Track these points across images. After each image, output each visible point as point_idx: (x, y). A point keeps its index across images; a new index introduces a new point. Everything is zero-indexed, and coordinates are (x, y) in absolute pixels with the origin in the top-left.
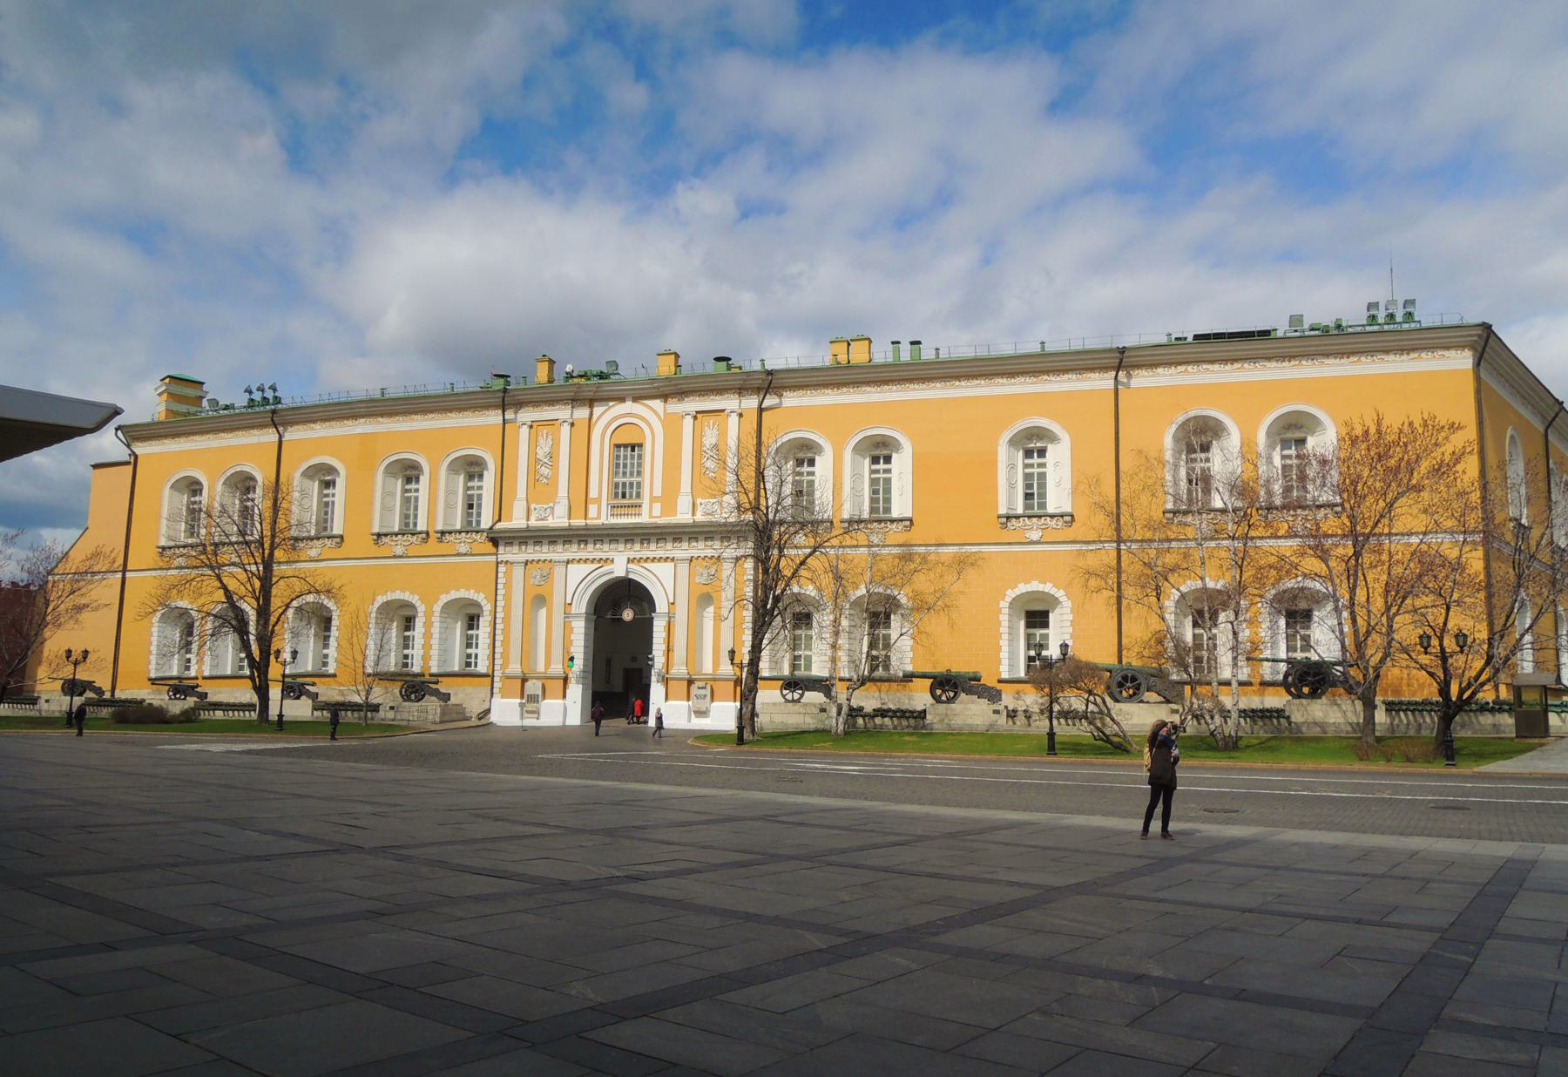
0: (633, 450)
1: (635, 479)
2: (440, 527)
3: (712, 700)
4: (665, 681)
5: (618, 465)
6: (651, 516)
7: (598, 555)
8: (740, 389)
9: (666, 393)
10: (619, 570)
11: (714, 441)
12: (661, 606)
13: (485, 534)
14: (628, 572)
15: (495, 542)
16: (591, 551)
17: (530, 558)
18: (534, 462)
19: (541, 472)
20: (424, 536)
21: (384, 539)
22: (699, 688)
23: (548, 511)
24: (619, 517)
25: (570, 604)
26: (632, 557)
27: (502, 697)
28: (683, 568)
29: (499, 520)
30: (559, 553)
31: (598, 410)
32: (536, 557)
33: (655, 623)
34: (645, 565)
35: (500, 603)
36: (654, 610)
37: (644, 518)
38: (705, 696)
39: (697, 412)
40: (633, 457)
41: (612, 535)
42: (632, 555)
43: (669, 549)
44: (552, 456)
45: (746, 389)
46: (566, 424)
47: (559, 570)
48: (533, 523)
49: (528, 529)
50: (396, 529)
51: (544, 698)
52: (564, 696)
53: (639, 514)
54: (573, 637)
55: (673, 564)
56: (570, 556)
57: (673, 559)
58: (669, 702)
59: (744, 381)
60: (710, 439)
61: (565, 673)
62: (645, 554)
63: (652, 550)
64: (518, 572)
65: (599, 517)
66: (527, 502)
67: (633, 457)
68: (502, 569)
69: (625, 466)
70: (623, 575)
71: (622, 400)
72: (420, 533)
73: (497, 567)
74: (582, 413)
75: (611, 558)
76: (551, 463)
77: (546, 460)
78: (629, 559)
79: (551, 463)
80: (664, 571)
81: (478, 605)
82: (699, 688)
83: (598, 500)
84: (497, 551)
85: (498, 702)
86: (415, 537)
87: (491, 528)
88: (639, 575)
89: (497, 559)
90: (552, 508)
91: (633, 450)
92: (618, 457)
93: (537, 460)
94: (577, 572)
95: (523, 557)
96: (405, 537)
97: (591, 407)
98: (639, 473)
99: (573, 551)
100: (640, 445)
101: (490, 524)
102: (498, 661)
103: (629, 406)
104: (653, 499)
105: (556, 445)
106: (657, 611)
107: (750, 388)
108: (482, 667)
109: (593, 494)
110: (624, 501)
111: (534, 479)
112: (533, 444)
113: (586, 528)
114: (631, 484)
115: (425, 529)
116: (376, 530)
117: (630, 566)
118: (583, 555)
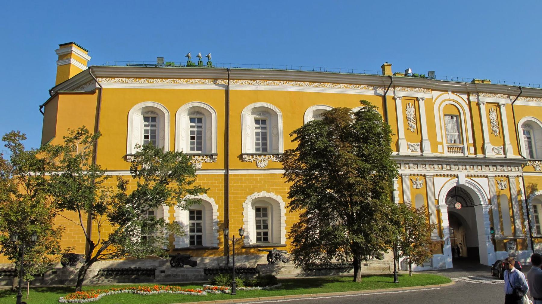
7: (449, 173)
9: (469, 91)
10: (463, 181)
16: (446, 170)
19: (411, 125)
30: (429, 171)
32: (416, 172)
43: (485, 171)
52: (443, 252)
56: (435, 173)
57: (487, 177)
58: (497, 252)
62: (473, 173)
63: (477, 170)
65: (443, 153)
80: (483, 182)
83: (441, 143)
99: (437, 170)
109: (439, 140)
112: (405, 109)
118: (442, 172)
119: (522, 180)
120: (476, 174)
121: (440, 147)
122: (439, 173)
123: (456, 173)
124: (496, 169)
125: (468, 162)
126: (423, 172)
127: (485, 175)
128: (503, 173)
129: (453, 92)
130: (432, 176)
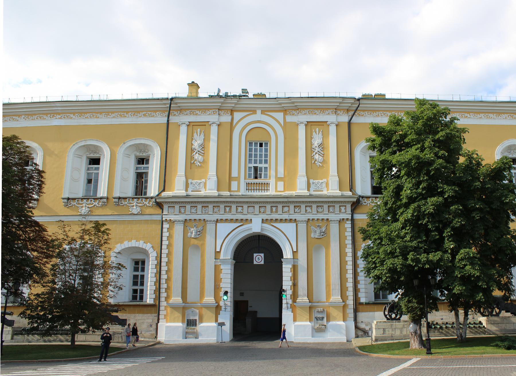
0: (261, 145)
1: (263, 165)
2: (117, 194)
3: (328, 320)
4: (293, 308)
5: (250, 155)
6: (276, 191)
7: (240, 217)
8: (336, 109)
11: (320, 141)
12: (287, 254)
13: (154, 200)
14: (262, 229)
15: (160, 205)
17: (188, 217)
18: (190, 150)
20: (105, 200)
21: (73, 203)
22: (318, 312)
23: (202, 185)
24: (258, 191)
25: (219, 252)
26: (265, 218)
27: (167, 322)
28: (303, 227)
29: (164, 190)
31: (237, 116)
32: (193, 217)
33: (284, 266)
34: (274, 224)
35: (165, 251)
36: (283, 257)
37: (272, 192)
38: (323, 318)
39: (307, 122)
40: (261, 151)
41: (251, 202)
42: (265, 217)
44: (203, 146)
45: (340, 110)
46: (214, 125)
47: (210, 227)
48: (190, 193)
49: (187, 196)
50: (80, 195)
51: (201, 321)
53: (267, 190)
54: (222, 276)
55: (295, 224)
56: (219, 217)
59: (338, 106)
60: (317, 141)
61: (216, 303)
62: (275, 216)
64: (179, 229)
65: (238, 190)
66: (186, 178)
67: (261, 151)
68: (166, 226)
69: (256, 156)
70: (259, 231)
71: (254, 112)
72: (101, 198)
73: (162, 224)
74: (226, 118)
75: (249, 218)
76: (203, 152)
77: (199, 150)
78: (263, 220)
79: (203, 152)
80: (289, 229)
81: (145, 252)
82: (318, 312)
83: (238, 179)
84: (163, 212)
85: (163, 325)
86: (98, 201)
87: (158, 196)
88: (271, 231)
89: (162, 218)
90: (205, 184)
91: (261, 145)
92: (250, 150)
93: (192, 150)
94: (224, 229)
95: (182, 217)
96: (89, 202)
97: (232, 114)
98: (266, 161)
100: (266, 144)
101: (157, 193)
102: (164, 295)
103: (258, 116)
104: (278, 179)
105: (207, 139)
106: (284, 257)
107: (342, 109)
108: (149, 299)
109: (234, 174)
110: (256, 181)
111: (190, 164)
113: (231, 196)
114: (261, 168)
115: (106, 195)
116: (67, 196)
117: (265, 225)
118: (229, 217)
119: (350, 226)
120: (279, 217)
121: (234, 185)
122: (224, 217)
123: (249, 217)
124: (311, 212)
125: (280, 202)
126: (202, 217)
127: (294, 218)
128: (320, 216)
129: (263, 112)
130: (213, 221)
